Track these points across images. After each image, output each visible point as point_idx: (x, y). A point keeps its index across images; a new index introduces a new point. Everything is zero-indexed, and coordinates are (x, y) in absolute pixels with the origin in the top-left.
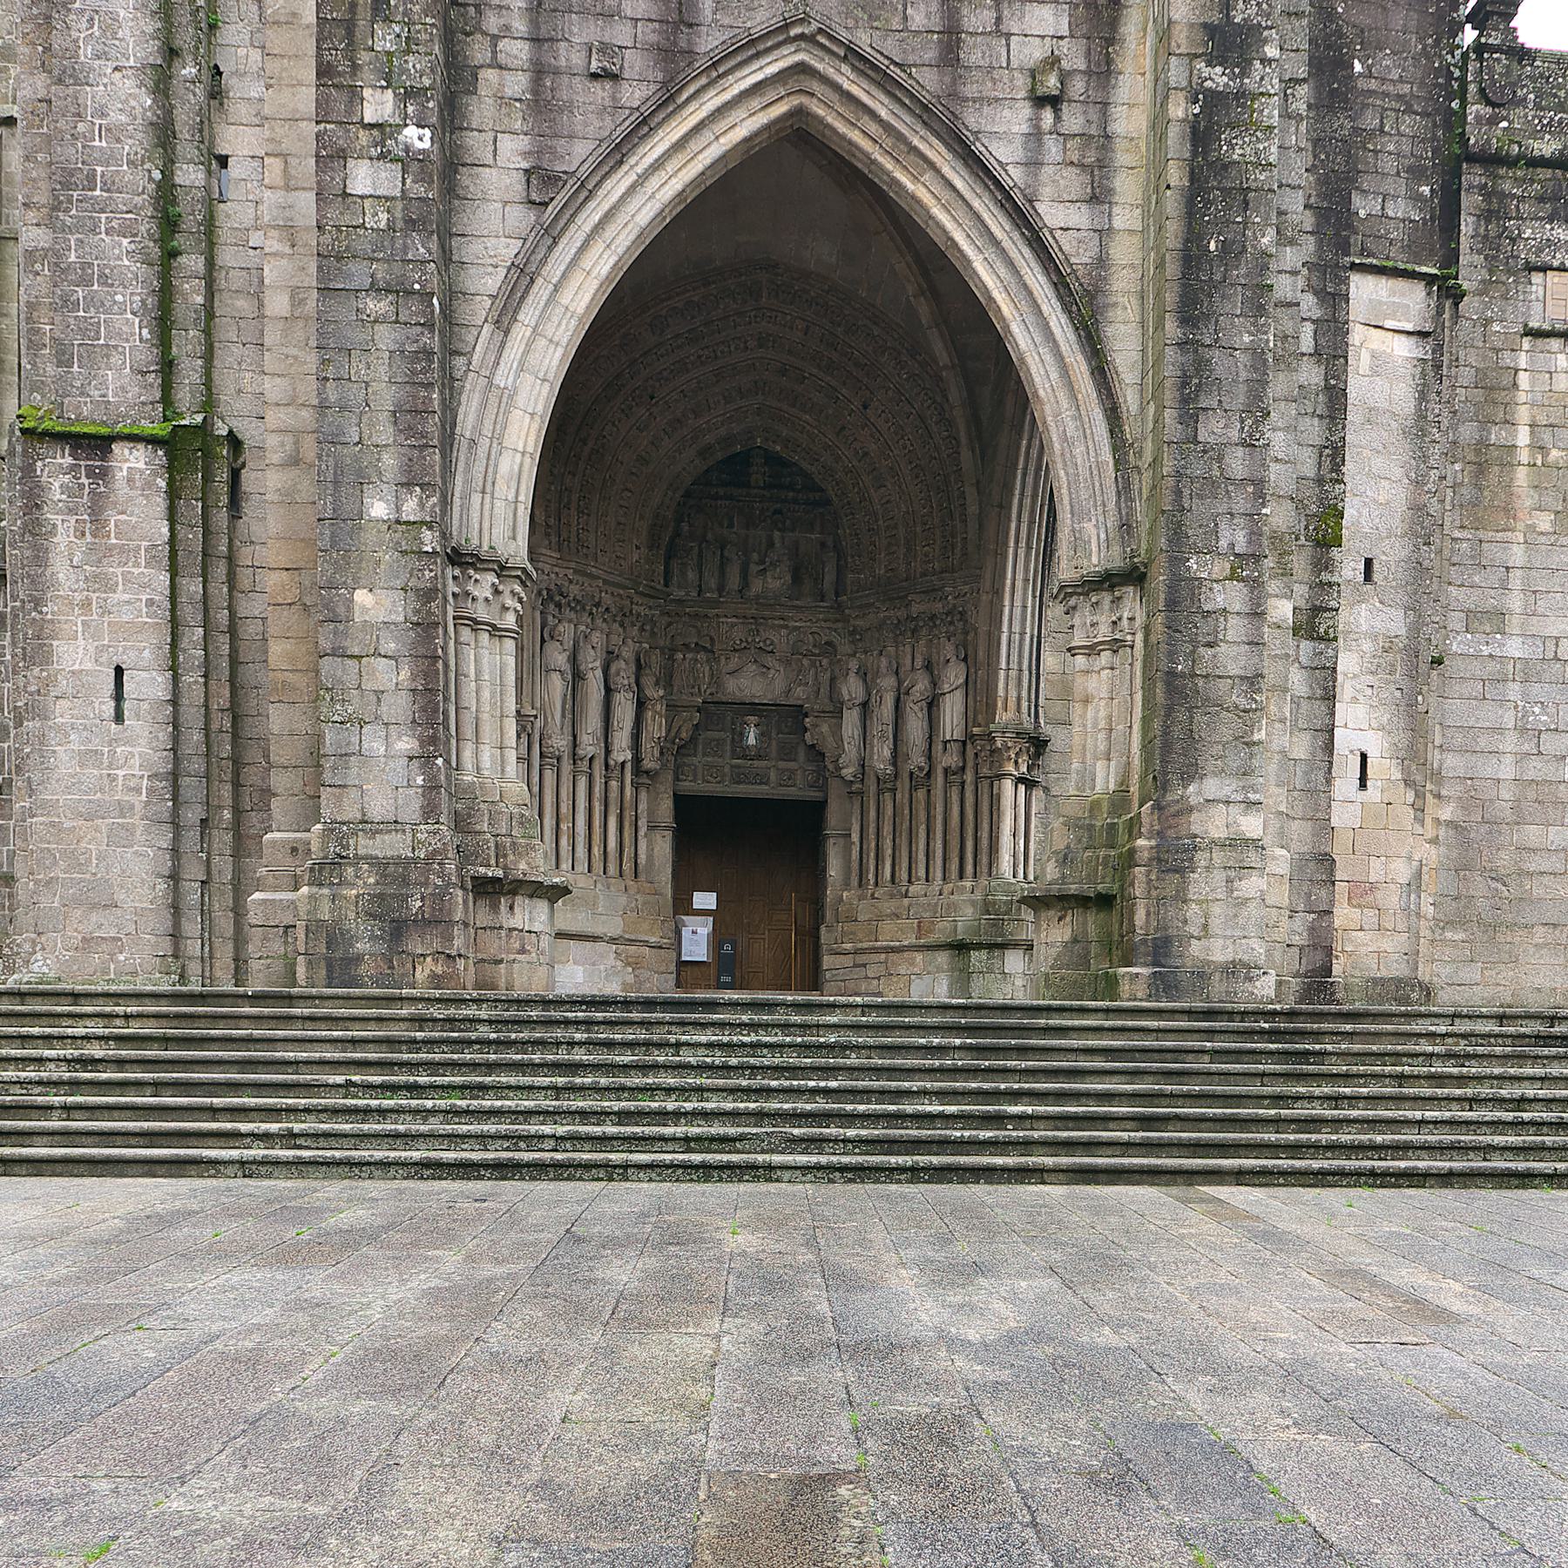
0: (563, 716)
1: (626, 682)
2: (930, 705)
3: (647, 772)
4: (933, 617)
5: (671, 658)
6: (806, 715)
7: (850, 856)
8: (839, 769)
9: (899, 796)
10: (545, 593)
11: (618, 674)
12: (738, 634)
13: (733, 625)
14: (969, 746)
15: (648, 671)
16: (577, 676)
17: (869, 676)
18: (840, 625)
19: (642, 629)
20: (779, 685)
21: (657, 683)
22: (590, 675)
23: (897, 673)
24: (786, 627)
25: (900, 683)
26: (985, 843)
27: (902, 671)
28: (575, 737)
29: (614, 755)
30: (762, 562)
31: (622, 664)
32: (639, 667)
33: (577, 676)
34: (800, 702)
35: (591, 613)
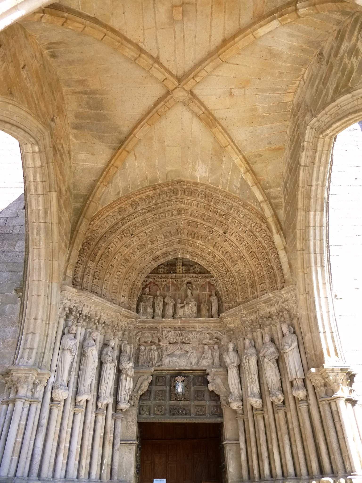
0: (69, 375)
1: (111, 358)
2: (277, 361)
3: (122, 410)
4: (270, 316)
5: (139, 349)
6: (208, 375)
7: (240, 457)
8: (228, 403)
9: (266, 417)
10: (67, 309)
11: (107, 354)
12: (171, 336)
13: (169, 332)
14: (308, 382)
15: (125, 354)
16: (82, 354)
17: (239, 352)
18: (221, 329)
19: (123, 334)
20: (194, 360)
21: (129, 360)
22: (89, 353)
23: (255, 347)
24: (195, 331)
25: (258, 353)
26: (335, 445)
27: (257, 346)
28: (77, 388)
29: (101, 399)
30: (182, 303)
31: (110, 349)
32: (121, 352)
33: (82, 354)
34: (204, 368)
35: (95, 324)
